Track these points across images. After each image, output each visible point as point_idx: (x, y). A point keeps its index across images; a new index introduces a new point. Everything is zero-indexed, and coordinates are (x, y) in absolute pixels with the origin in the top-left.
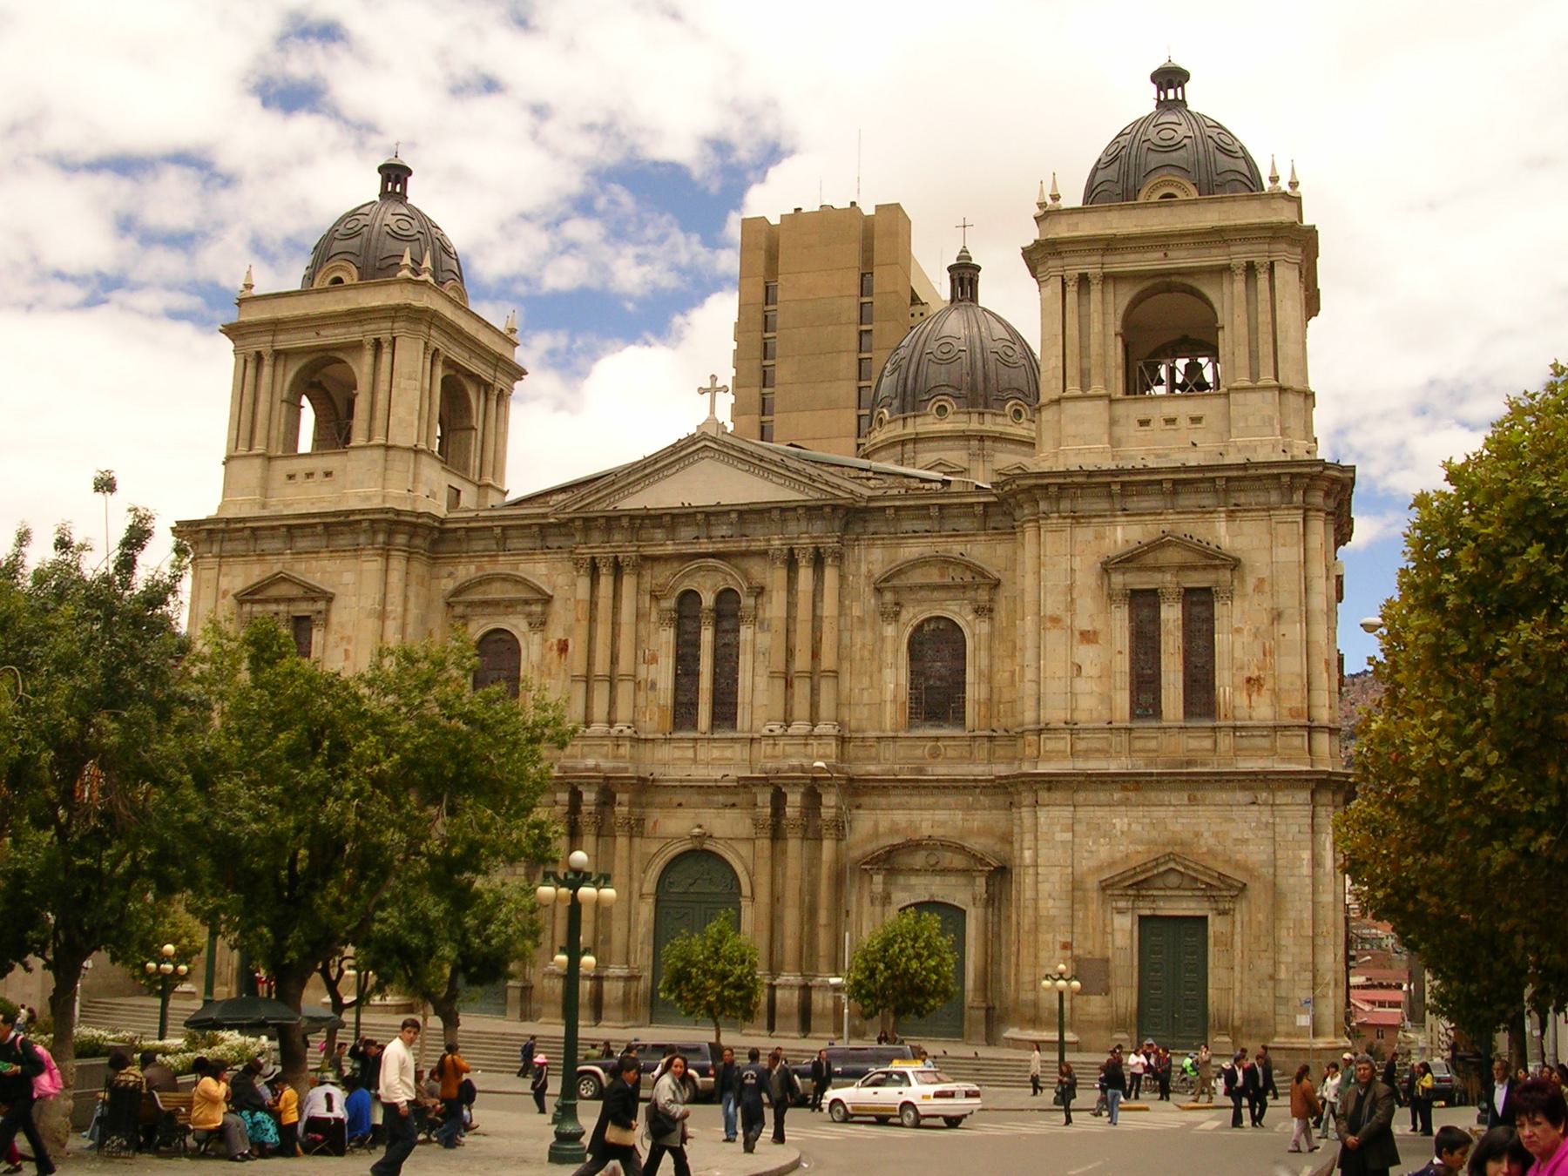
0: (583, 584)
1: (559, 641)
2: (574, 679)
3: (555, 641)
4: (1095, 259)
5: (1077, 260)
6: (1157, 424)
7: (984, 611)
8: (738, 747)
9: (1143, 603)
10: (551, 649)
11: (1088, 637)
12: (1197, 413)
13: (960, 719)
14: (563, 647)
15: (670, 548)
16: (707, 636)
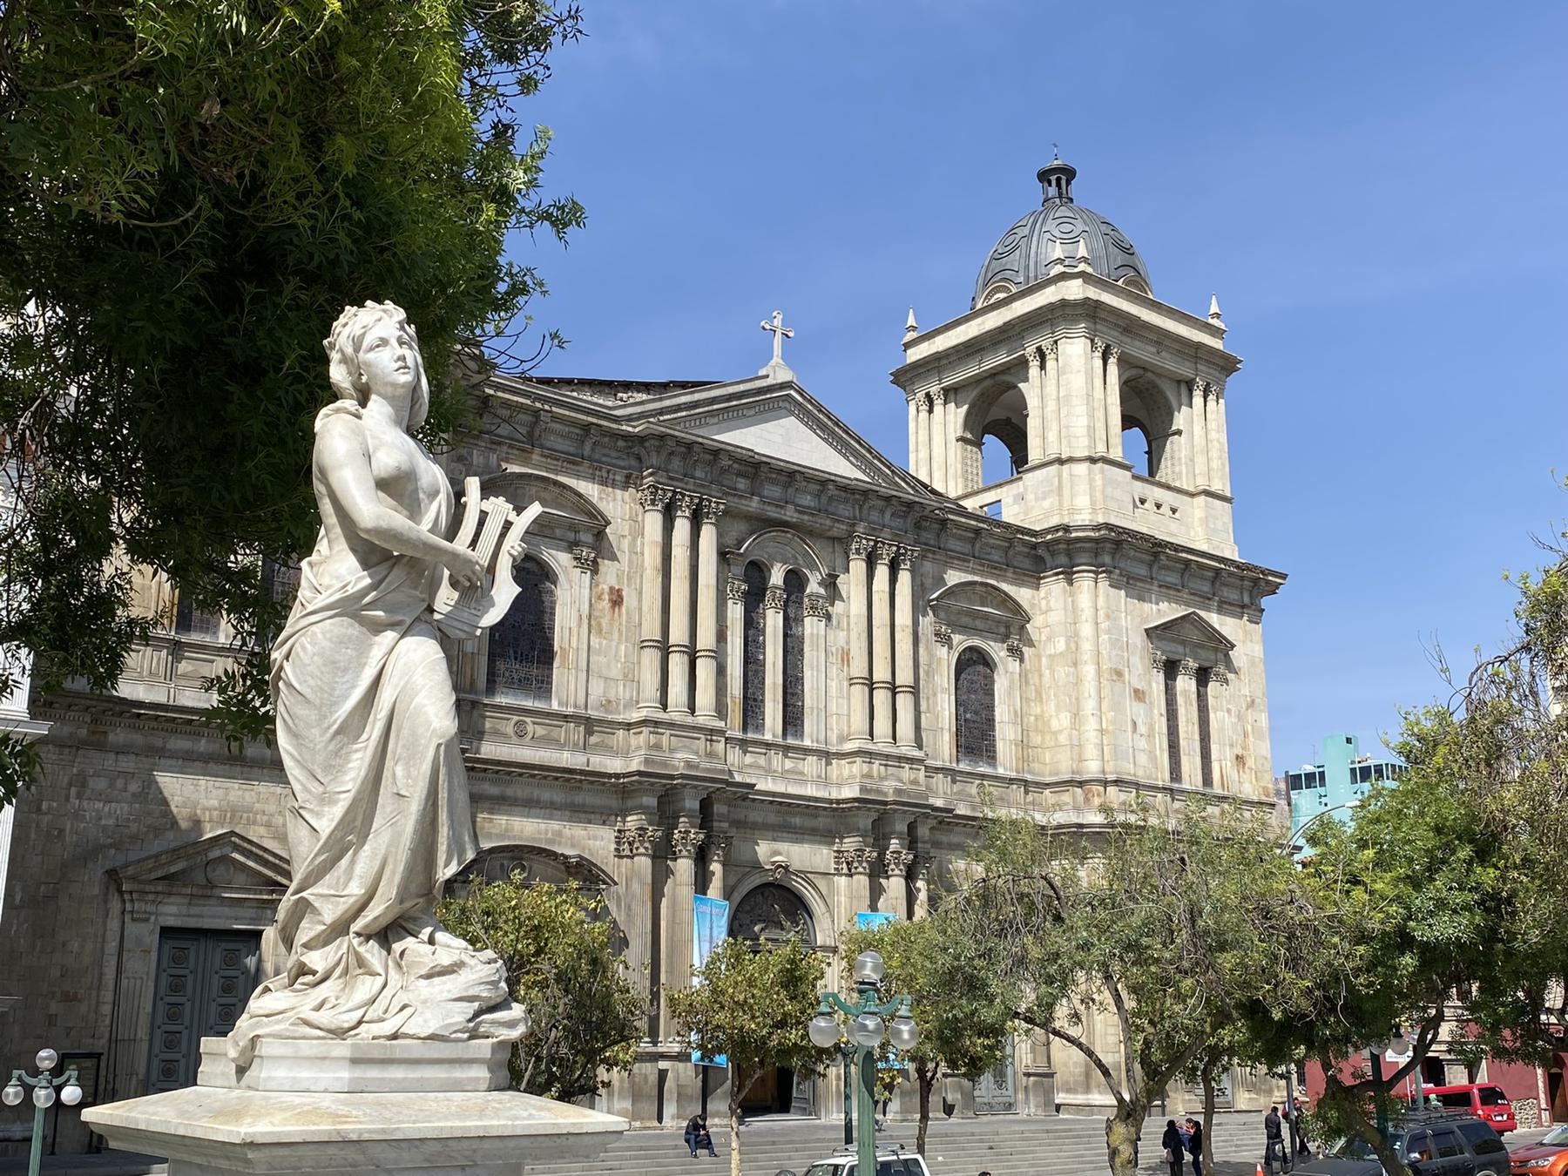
0: (654, 521)
1: (611, 589)
2: (643, 645)
3: (607, 589)
4: (1116, 334)
5: (1105, 329)
6: (1149, 505)
7: (1015, 652)
8: (811, 759)
9: (1171, 669)
10: (600, 598)
11: (1139, 695)
12: (1175, 505)
13: (990, 755)
14: (617, 600)
15: (754, 504)
16: (773, 621)
